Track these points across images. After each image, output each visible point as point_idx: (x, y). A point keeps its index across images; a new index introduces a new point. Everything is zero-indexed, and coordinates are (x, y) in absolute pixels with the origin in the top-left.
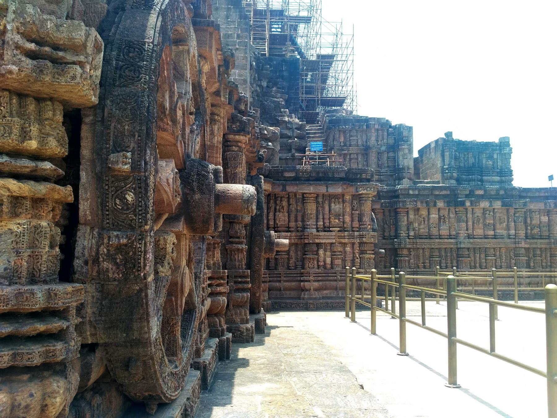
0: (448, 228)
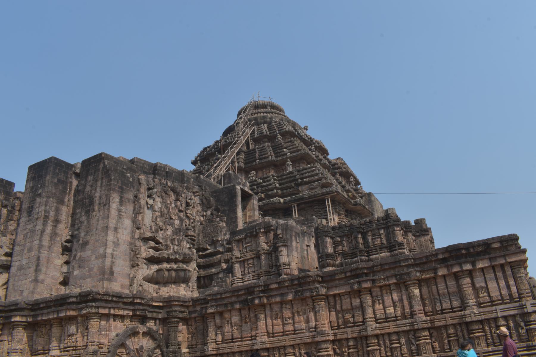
0: (249, 328)
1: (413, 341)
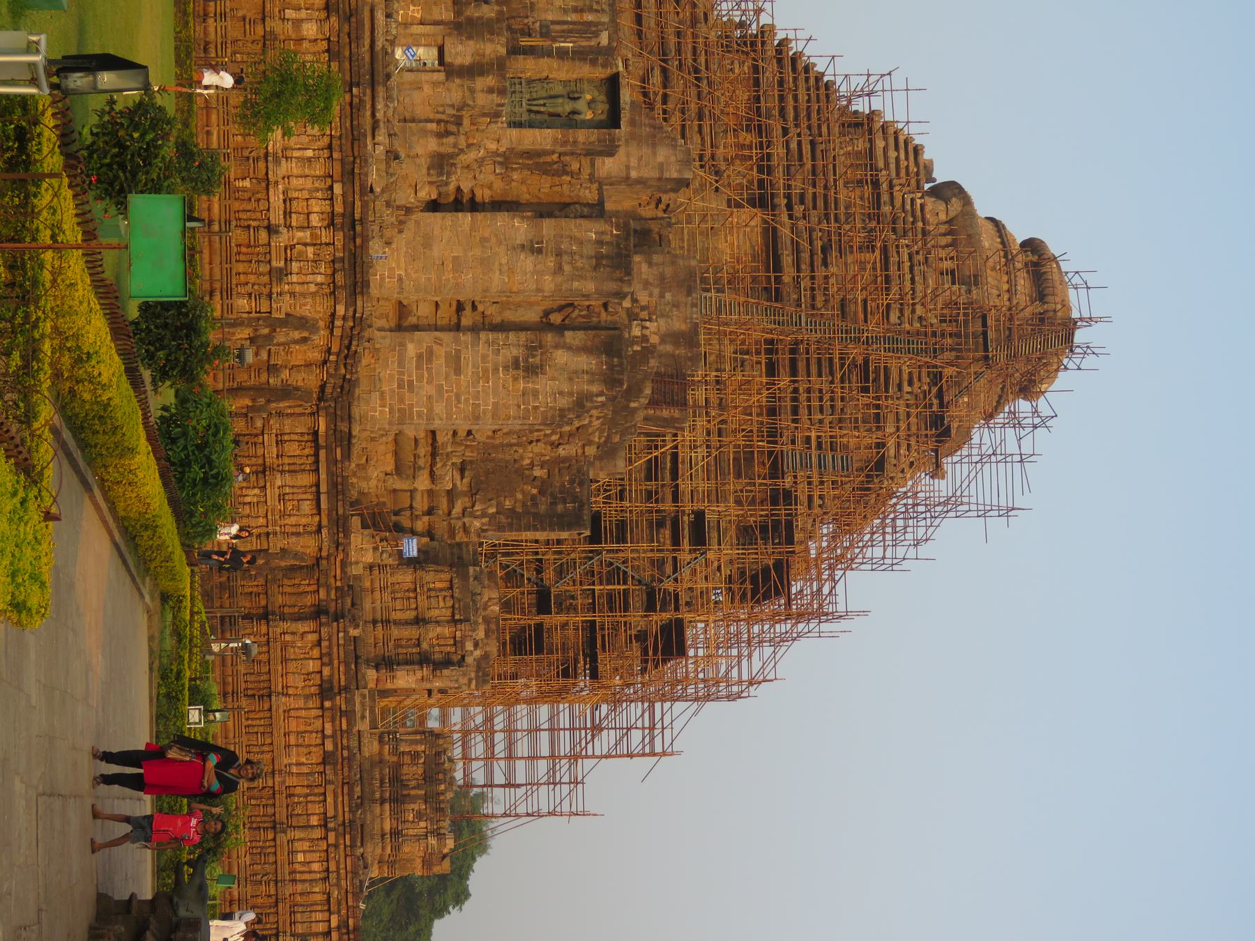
1: (265, 878)
